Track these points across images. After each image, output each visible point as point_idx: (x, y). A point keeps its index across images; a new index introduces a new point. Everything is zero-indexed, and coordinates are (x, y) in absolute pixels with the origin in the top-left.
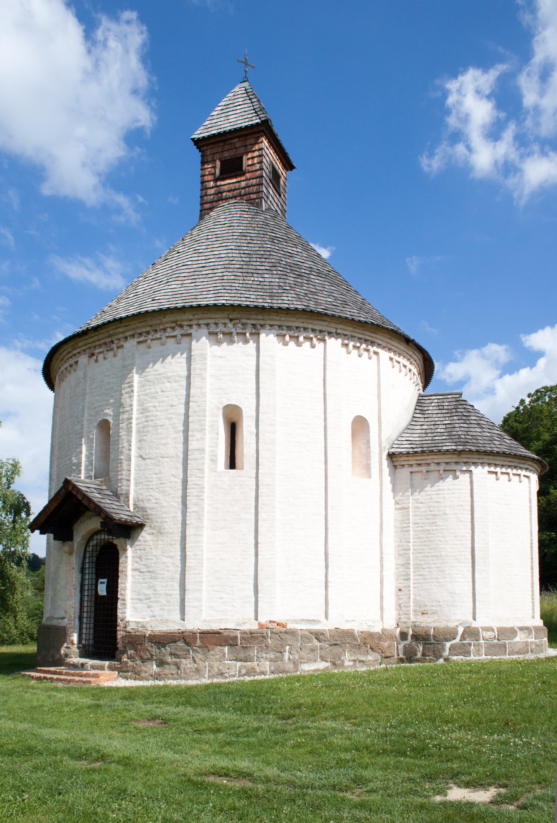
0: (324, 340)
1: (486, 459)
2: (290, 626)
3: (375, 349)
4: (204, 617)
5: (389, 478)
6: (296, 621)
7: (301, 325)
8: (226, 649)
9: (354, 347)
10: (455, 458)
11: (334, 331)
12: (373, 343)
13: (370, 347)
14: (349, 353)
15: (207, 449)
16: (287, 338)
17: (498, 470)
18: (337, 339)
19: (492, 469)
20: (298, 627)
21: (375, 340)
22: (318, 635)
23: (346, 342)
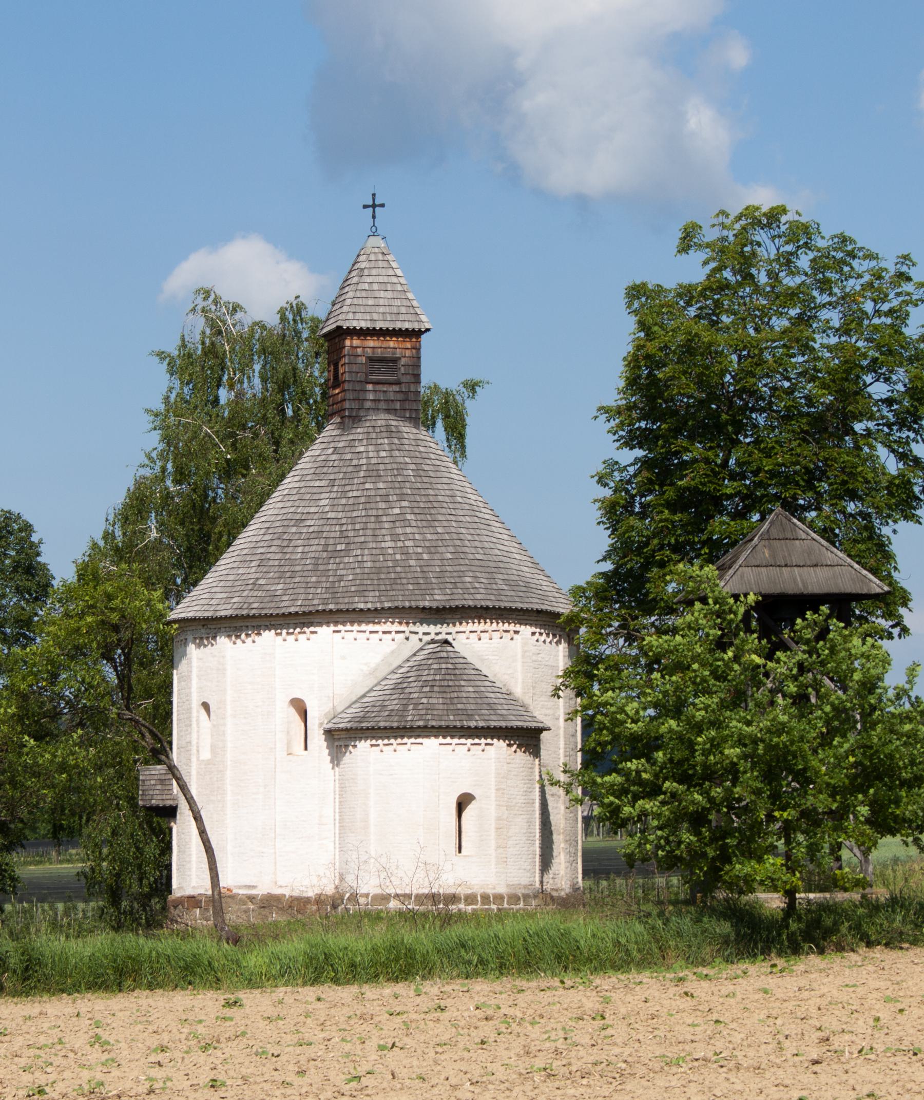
0: (260, 634)
1: (368, 733)
2: (235, 891)
3: (312, 629)
4: (194, 883)
5: (327, 751)
6: (240, 887)
7: (242, 624)
8: (198, 910)
9: (288, 633)
10: (343, 735)
11: (268, 624)
12: (311, 624)
13: (305, 629)
14: (285, 640)
15: (194, 742)
16: (233, 638)
17: (380, 742)
18: (270, 630)
19: (374, 742)
20: (241, 892)
21: (312, 620)
22: (251, 898)
23: (279, 631)
